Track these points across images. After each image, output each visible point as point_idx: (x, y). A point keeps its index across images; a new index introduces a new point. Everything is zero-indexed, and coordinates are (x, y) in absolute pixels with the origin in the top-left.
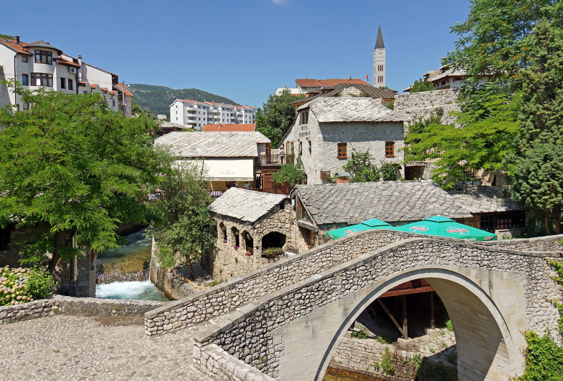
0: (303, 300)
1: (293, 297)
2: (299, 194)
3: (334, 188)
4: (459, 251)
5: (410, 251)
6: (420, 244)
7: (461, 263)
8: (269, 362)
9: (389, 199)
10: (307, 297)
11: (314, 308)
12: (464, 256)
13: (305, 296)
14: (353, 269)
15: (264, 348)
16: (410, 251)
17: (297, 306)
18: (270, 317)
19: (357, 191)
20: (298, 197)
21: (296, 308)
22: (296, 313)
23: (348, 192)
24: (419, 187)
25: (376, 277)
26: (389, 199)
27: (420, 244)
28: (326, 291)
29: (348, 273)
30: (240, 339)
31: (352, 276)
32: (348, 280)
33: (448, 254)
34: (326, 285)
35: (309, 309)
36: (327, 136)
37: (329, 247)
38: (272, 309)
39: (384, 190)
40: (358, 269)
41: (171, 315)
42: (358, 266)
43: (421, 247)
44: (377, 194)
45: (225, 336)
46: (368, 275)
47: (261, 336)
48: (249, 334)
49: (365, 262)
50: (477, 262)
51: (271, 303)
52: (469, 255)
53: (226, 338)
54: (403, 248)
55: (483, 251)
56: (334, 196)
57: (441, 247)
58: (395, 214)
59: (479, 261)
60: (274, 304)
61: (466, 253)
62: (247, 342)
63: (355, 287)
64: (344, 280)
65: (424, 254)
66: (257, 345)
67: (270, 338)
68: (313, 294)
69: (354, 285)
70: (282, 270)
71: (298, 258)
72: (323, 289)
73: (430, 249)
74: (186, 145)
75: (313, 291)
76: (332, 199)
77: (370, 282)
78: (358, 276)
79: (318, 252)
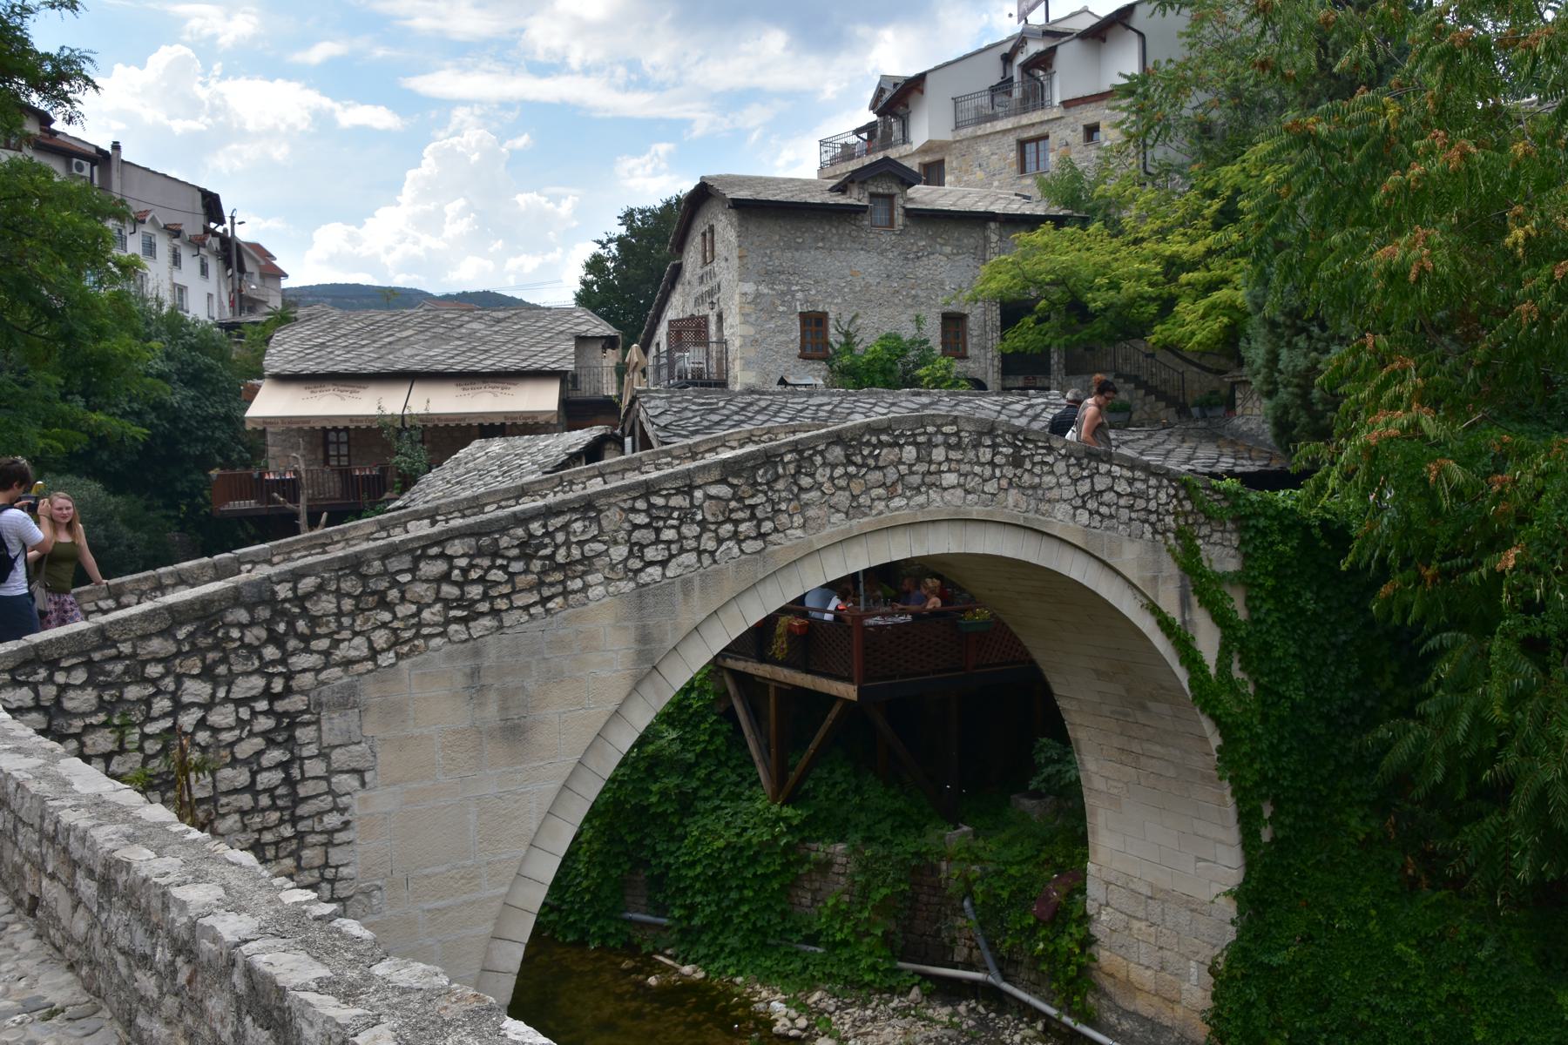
0: (455, 583)
1: (413, 570)
2: (642, 415)
3: (759, 400)
4: (1085, 474)
5: (910, 453)
6: (946, 429)
7: (1091, 513)
8: (303, 810)
10: (474, 575)
11: (508, 619)
12: (1101, 492)
13: (465, 571)
14: (678, 491)
15: (276, 755)
16: (910, 453)
17: (429, 606)
18: (306, 639)
19: (831, 412)
20: (641, 423)
21: (426, 615)
22: (425, 631)
23: (801, 411)
24: (1019, 407)
25: (776, 530)
27: (946, 429)
28: (560, 557)
29: (659, 501)
30: (147, 702)
31: (675, 514)
32: (658, 531)
33: (1049, 480)
34: (560, 537)
35: (487, 622)
36: (766, 291)
37: (637, 464)
38: (316, 608)
40: (698, 494)
42: (699, 481)
43: (953, 440)
45: (60, 678)
46: (743, 520)
47: (262, 705)
48: (196, 690)
49: (729, 470)
50: (1142, 515)
51: (308, 584)
52: (1119, 490)
53: (63, 688)
54: (884, 438)
55: (1165, 482)
56: (754, 422)
57: (1024, 452)
59: (1150, 512)
60: (321, 588)
61: (1108, 481)
62: (188, 720)
63: (689, 558)
64: (636, 527)
65: (965, 468)
66: (240, 739)
67: (306, 717)
68: (504, 568)
69: (682, 550)
71: (507, 490)
72: (547, 551)
73: (986, 454)
74: (363, 343)
75: (503, 557)
77: (750, 546)
78: (699, 517)
79: (590, 478)
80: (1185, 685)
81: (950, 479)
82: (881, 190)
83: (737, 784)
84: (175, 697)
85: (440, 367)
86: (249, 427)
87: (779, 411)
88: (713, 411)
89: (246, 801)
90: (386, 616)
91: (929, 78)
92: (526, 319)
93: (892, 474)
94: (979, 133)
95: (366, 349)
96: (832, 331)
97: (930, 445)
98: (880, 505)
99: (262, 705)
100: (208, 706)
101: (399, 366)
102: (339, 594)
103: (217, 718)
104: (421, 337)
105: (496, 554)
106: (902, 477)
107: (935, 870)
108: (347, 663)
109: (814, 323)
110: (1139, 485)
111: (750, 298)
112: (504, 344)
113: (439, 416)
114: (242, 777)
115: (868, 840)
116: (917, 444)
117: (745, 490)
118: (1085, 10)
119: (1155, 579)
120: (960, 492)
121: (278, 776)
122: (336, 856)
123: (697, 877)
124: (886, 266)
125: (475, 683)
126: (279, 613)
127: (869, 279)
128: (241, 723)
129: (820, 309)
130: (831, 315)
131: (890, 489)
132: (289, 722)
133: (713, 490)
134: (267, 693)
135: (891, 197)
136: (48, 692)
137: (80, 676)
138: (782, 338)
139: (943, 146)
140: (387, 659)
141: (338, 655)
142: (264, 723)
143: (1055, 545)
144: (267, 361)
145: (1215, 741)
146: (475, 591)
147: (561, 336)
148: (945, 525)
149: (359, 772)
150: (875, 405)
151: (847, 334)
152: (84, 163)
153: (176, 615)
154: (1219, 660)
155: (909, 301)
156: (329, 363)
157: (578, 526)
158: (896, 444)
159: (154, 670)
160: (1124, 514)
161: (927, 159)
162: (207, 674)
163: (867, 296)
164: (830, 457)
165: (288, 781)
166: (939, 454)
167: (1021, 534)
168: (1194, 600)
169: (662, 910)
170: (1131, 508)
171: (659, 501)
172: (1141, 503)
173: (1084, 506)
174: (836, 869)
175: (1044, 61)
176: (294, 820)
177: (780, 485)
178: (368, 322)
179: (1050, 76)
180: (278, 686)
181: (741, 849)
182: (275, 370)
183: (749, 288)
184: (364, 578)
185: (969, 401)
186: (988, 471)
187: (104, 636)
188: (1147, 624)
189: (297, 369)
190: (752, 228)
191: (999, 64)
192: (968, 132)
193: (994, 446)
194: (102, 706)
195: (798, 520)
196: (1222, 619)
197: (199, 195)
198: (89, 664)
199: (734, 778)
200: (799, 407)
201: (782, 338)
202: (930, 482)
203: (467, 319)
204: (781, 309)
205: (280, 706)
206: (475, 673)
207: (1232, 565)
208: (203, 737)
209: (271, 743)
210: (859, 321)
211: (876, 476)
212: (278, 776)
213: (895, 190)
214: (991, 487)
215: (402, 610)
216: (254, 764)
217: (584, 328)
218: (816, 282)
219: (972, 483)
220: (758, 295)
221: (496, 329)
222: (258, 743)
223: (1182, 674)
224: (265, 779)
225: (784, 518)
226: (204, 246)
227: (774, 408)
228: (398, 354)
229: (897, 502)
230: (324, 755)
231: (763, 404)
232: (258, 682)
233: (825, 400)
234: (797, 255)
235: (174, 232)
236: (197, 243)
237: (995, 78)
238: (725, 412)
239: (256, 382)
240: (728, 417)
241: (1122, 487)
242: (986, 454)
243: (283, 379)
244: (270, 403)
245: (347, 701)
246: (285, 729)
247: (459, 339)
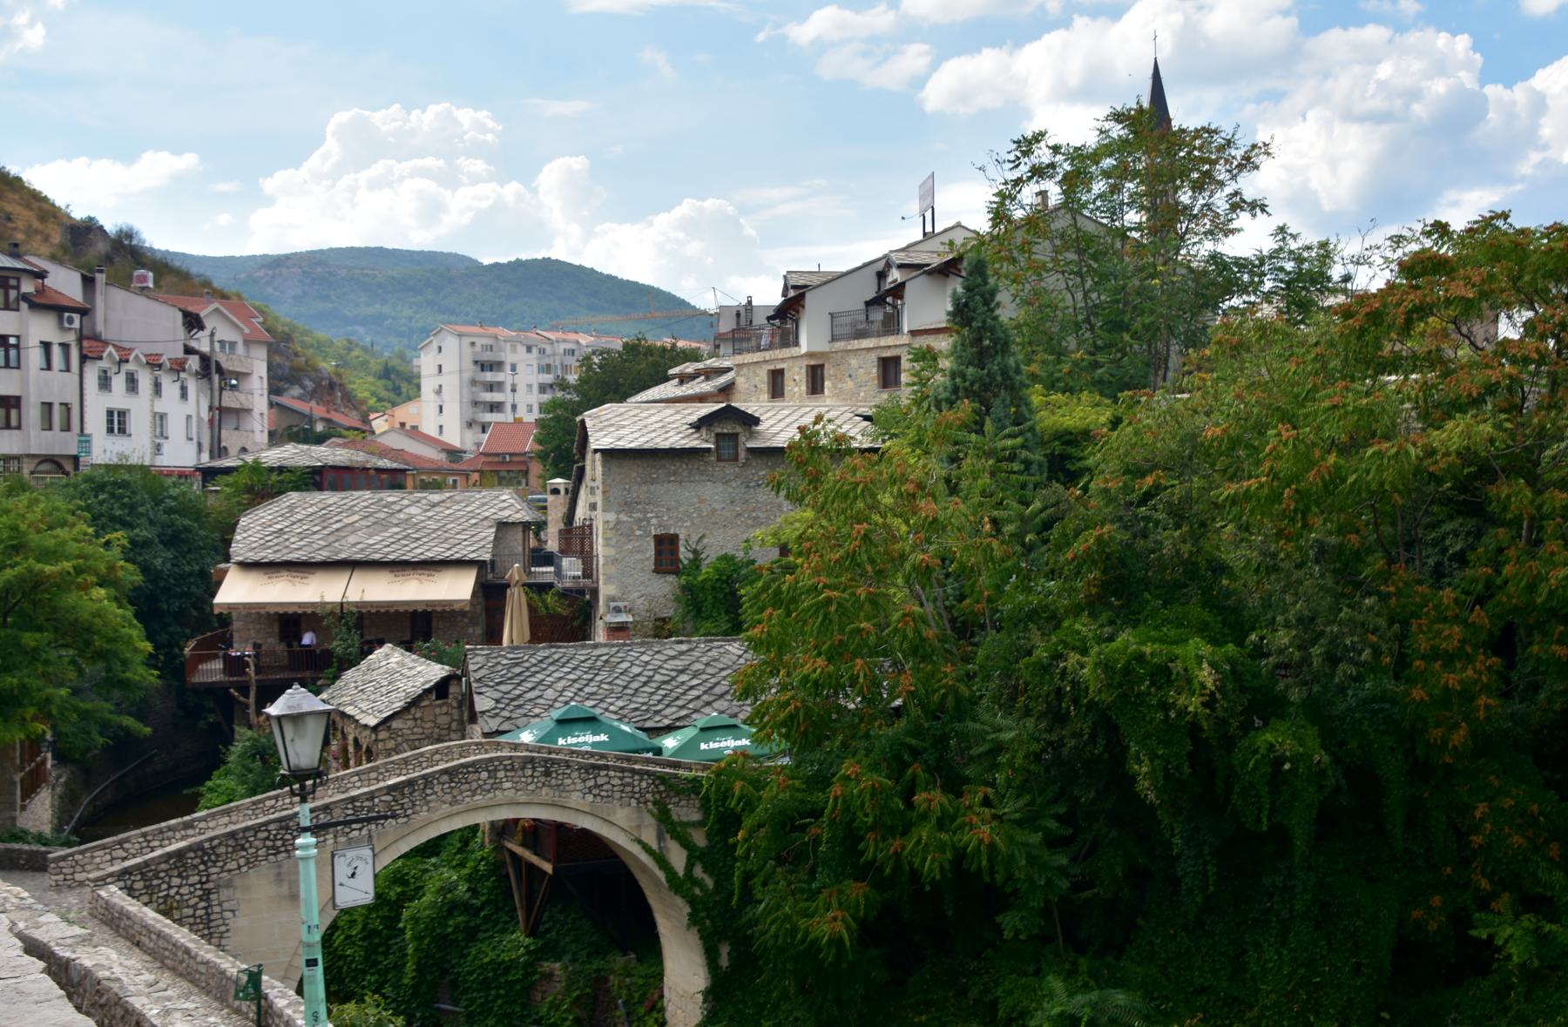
1: (255, 836)
5: (484, 775)
8: (212, 924)
9: (673, 678)
15: (203, 904)
18: (215, 862)
19: (606, 661)
21: (260, 853)
26: (673, 678)
29: (358, 804)
30: (159, 885)
33: (568, 781)
35: (284, 855)
36: (625, 519)
39: (673, 658)
40: (376, 800)
41: (86, 860)
44: (650, 667)
48: (176, 881)
51: (216, 842)
58: (669, 711)
60: (220, 844)
61: (607, 779)
65: (516, 779)
70: (280, 803)
73: (529, 772)
76: (540, 677)
77: (401, 820)
80: (664, 880)
81: (508, 785)
82: (725, 431)
83: (506, 923)
84: (168, 883)
85: (376, 556)
86: (216, 611)
87: (568, 662)
88: (517, 665)
89: (192, 920)
90: (244, 853)
91: (809, 297)
92: (458, 502)
93: (474, 785)
94: (849, 348)
95: (316, 536)
96: (682, 549)
97: (496, 770)
98: (468, 799)
99: (198, 886)
100: (180, 887)
101: (342, 556)
102: (227, 846)
103: (183, 891)
104: (365, 523)
105: (287, 828)
106: (480, 786)
107: (606, 980)
108: (230, 871)
109: (666, 545)
110: (627, 780)
111: (611, 525)
112: (436, 530)
113: (372, 604)
114: (190, 912)
115: (574, 960)
116: (489, 771)
117: (399, 797)
118: (959, 225)
119: (639, 827)
120: (513, 791)
121: (203, 912)
122: (224, 942)
123: (474, 981)
124: (730, 494)
125: (279, 878)
126: (205, 853)
127: (715, 505)
128: (191, 893)
129: (672, 532)
130: (681, 537)
131: (474, 792)
132: (208, 893)
133: (383, 798)
134: (200, 882)
135: (735, 436)
136: (129, 882)
137: (139, 877)
138: (639, 556)
139: (822, 355)
140: (244, 869)
141: (226, 868)
142: (199, 893)
143: (573, 812)
144: (234, 548)
145: (688, 910)
146: (279, 843)
147: (486, 523)
148: (505, 807)
149: (233, 911)
150: (644, 653)
151: (695, 552)
152: (74, 315)
153: (170, 855)
154: (686, 868)
155: (750, 522)
156: (285, 551)
157: (322, 816)
158: (476, 772)
159: (162, 875)
160: (617, 795)
161: (812, 363)
162: (180, 875)
163: (713, 520)
164: (441, 780)
165: (207, 914)
166: (501, 774)
167: (551, 808)
168: (668, 836)
169: (456, 1002)
170: (622, 791)
171: (358, 804)
172: (628, 789)
173: (590, 792)
174: (555, 978)
175: (898, 291)
176: (209, 928)
177: (416, 794)
178: (321, 506)
179: (903, 305)
180: (204, 879)
181: (500, 964)
182: (240, 559)
183: (611, 517)
184: (236, 839)
185: (721, 646)
186: (530, 780)
187: (146, 864)
188: (635, 849)
189: (257, 558)
190: (614, 468)
191: (874, 280)
192: (840, 345)
193: (534, 769)
194: (146, 887)
195: (425, 808)
196: (686, 843)
197: (180, 315)
198: (142, 873)
199: (506, 918)
200: (582, 658)
201: (639, 556)
202: (496, 786)
203: (406, 502)
204: (638, 533)
205: (205, 886)
206: (279, 874)
207: (696, 816)
208: (178, 897)
209: (201, 900)
210: (705, 541)
211: (467, 786)
212: (203, 912)
213: (739, 429)
214: (531, 787)
215: (251, 851)
216: (195, 907)
217: (506, 513)
218: (669, 509)
219: (519, 786)
220: (618, 522)
221: (429, 514)
222: (197, 900)
223: (661, 875)
224: (199, 913)
225: (418, 808)
226: (184, 370)
227: (563, 660)
228: (343, 542)
229: (477, 798)
230: (220, 904)
231: (556, 657)
232: (197, 878)
233: (605, 650)
234: (652, 488)
235: (154, 364)
236: (178, 367)
237: (871, 293)
238: (527, 665)
239: (223, 566)
240: (528, 669)
241: (616, 781)
242: (529, 772)
243: (248, 566)
244: (236, 590)
245: (229, 884)
246: (206, 895)
247: (397, 525)
